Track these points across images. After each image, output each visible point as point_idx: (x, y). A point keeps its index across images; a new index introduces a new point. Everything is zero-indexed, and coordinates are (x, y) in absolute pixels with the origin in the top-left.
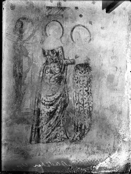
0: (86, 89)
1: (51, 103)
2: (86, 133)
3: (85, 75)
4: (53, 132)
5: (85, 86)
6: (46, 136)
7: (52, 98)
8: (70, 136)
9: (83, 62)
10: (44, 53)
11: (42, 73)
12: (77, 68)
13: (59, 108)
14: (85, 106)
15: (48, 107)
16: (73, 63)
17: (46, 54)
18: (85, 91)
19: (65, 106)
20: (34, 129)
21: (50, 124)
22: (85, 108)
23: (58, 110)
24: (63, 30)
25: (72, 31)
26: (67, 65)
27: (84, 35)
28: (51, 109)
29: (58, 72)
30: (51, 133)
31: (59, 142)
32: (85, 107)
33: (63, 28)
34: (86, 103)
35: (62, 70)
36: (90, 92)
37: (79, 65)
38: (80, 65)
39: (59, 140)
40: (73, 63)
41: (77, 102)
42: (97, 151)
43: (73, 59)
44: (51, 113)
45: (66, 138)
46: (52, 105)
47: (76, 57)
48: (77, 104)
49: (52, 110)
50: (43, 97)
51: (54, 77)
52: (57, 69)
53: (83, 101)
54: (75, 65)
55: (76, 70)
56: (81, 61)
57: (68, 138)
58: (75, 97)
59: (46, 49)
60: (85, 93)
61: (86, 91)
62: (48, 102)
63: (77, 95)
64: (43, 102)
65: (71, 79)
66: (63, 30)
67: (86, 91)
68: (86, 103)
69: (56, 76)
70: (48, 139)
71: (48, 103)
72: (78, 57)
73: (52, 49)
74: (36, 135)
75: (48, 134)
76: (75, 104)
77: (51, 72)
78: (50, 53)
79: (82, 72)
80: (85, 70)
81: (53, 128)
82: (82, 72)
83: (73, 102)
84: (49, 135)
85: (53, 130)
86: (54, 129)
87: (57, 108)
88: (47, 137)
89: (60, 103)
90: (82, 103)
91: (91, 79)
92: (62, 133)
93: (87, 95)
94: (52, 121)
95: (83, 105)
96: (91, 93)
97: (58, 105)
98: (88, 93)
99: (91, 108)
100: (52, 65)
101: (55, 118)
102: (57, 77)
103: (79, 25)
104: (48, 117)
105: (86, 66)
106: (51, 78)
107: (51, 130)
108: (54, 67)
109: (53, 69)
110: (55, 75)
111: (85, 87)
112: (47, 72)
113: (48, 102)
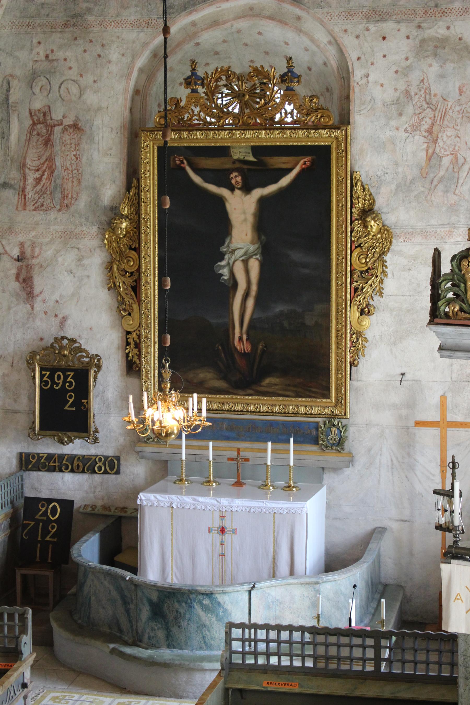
0: (75, 153)
1: (37, 168)
2: (73, 202)
3: (74, 137)
4: (40, 200)
5: (72, 149)
6: (33, 204)
7: (37, 163)
8: (57, 205)
9: (72, 123)
10: (31, 113)
11: (28, 135)
12: (64, 130)
13: (46, 174)
14: (74, 172)
15: (33, 172)
16: (60, 124)
17: (33, 114)
18: (72, 156)
19: (52, 172)
20: (20, 195)
21: (36, 191)
22: (74, 175)
23: (45, 177)
24: (50, 86)
25: (60, 87)
26: (54, 126)
27: (74, 90)
28: (37, 175)
29: (45, 134)
30: (37, 201)
31: (46, 210)
32: (75, 174)
33: (50, 84)
34: (75, 169)
35: (49, 132)
36: (78, 157)
37: (67, 125)
38: (69, 126)
39: (45, 209)
40: (60, 124)
41: (65, 168)
42: (85, 223)
43: (61, 120)
44: (37, 179)
45: (53, 206)
46: (38, 170)
47: (64, 117)
48: (65, 170)
49: (38, 176)
50: (28, 162)
51: (41, 139)
52: (45, 131)
53: (72, 166)
54: (63, 126)
55: (63, 132)
56: (68, 121)
57: (55, 207)
58: (62, 162)
59: (32, 108)
60: (74, 158)
61: (74, 155)
62: (34, 167)
63: (64, 159)
64: (29, 166)
65: (58, 142)
66: (50, 86)
67: (74, 155)
68: (75, 169)
69: (43, 138)
70: (34, 206)
71: (34, 168)
72: (66, 117)
73: (38, 108)
74: (23, 202)
75: (35, 202)
76: (63, 171)
77: (38, 134)
78: (37, 113)
79: (71, 134)
80: (74, 131)
81: (39, 196)
82: (71, 134)
83: (60, 168)
84: (36, 203)
85: (39, 198)
86: (41, 196)
87: (43, 175)
88: (34, 205)
89: (46, 167)
90: (71, 169)
91: (79, 142)
92: (49, 201)
93: (75, 160)
94: (39, 187)
95: (72, 172)
96: (79, 158)
97: (44, 171)
98: (77, 159)
99: (80, 175)
100: (39, 126)
101: (42, 184)
102: (44, 140)
103: (67, 80)
104: (35, 183)
105: (75, 127)
106: (38, 140)
107: (37, 198)
108: (41, 128)
109: (40, 131)
110: (42, 137)
111: (73, 151)
112: (33, 134)
113: (34, 167)
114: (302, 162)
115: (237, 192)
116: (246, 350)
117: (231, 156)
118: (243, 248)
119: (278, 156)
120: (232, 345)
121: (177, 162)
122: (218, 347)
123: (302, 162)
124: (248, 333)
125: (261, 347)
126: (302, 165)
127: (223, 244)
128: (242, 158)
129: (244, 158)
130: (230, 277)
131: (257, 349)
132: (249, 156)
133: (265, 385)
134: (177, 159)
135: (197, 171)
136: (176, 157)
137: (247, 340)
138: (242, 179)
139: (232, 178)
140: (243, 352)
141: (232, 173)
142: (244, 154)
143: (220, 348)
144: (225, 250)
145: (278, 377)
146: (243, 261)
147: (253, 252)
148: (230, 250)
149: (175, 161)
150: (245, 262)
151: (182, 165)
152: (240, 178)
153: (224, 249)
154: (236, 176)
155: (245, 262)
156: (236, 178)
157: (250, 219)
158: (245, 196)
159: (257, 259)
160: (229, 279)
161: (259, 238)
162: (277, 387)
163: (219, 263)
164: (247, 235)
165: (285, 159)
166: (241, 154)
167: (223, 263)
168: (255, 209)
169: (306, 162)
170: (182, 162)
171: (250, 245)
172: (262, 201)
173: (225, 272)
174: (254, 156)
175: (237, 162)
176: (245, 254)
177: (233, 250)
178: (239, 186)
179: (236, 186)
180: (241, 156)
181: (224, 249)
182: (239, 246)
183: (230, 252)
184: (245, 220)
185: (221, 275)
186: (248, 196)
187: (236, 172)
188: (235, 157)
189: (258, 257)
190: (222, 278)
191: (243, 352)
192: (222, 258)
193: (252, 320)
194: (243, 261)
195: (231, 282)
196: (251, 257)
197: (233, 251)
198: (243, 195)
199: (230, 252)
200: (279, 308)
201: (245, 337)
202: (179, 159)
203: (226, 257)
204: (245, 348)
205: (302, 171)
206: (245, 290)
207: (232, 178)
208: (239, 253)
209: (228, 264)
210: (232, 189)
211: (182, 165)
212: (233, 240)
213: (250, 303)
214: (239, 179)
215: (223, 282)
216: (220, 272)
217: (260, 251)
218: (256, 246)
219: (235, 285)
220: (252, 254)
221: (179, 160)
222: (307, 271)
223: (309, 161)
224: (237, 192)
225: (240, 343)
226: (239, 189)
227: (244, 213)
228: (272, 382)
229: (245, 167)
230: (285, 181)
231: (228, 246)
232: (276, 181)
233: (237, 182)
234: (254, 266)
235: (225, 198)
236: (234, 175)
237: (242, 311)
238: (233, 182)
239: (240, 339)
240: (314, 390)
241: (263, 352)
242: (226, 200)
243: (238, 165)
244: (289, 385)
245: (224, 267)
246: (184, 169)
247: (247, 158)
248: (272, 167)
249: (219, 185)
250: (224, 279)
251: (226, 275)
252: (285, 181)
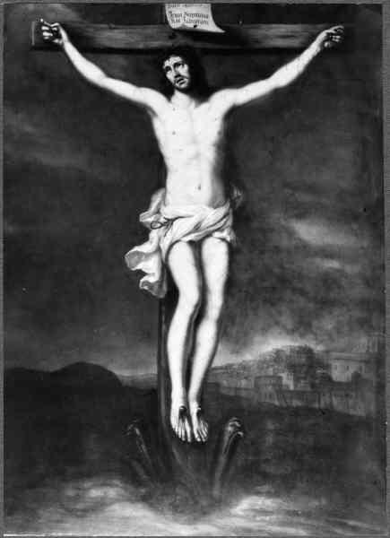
114: (323, 36)
115: (179, 98)
116: (196, 436)
117: (167, 23)
118: (190, 216)
119: (269, 22)
120: (165, 425)
121: (45, 34)
122: (133, 430)
123: (323, 36)
124: (201, 399)
125: (230, 429)
126: (324, 41)
127: (146, 206)
128: (191, 26)
129: (195, 26)
130: (162, 276)
131: (221, 433)
132: (207, 23)
133: (241, 513)
134: (44, 28)
135: (87, 50)
136: (43, 24)
137: (199, 414)
138: (190, 71)
139: (168, 68)
140: (189, 440)
141: (168, 58)
142: (195, 18)
143: (138, 431)
144: (151, 220)
145: (269, 495)
146: (191, 243)
147: (215, 224)
148: (162, 220)
149: (39, 32)
150: (196, 246)
151: (56, 41)
152: (186, 67)
153: (147, 218)
154: (176, 65)
155: (196, 246)
156: (177, 69)
157: (209, 155)
158: (196, 106)
159: (223, 240)
160: (160, 283)
161: (228, 195)
162: (268, 518)
163: (136, 249)
164: (200, 188)
165: (283, 29)
166: (187, 18)
167: (146, 248)
168: (219, 133)
169: (332, 34)
170: (58, 36)
171: (208, 209)
172: (234, 116)
173: (151, 269)
174: (218, 25)
175: (179, 36)
176: (197, 228)
177: (168, 220)
178: (183, 86)
179: (177, 85)
180: (190, 22)
181: (147, 218)
182: (182, 213)
183: (162, 225)
184: (197, 156)
185: (141, 274)
186: (205, 106)
187: (177, 55)
188: (174, 25)
189: (225, 234)
190: (142, 280)
191: (189, 440)
192: (142, 235)
193: (209, 371)
194: (191, 243)
195: (165, 288)
196: (209, 235)
197: (169, 223)
198: (193, 104)
199: (162, 225)
200: (272, 344)
201: (194, 408)
202: (50, 27)
203: (154, 235)
204: (195, 432)
205: (323, 53)
206: (196, 306)
207: (168, 68)
208: (180, 228)
209: (159, 250)
210: (167, 90)
211: (56, 41)
212: (169, 197)
213: (207, 332)
214: (184, 70)
215: (146, 288)
216: (139, 267)
217: (230, 223)
218: (222, 211)
219: (173, 294)
220: (212, 229)
221: (50, 31)
222: (334, 264)
223: (338, 34)
224: (179, 98)
225: (183, 421)
226: (184, 91)
227: (195, 141)
228: (257, 507)
229: (198, 45)
230: (286, 75)
231: (158, 212)
232: (265, 74)
233: (178, 75)
234: (217, 256)
235: (150, 109)
236: (170, 62)
237: (189, 352)
238: (171, 76)
239: (184, 413)
240: (351, 523)
241: (236, 441)
242: (154, 113)
243: (181, 41)
244: (295, 513)
245: (148, 256)
246: (60, 48)
247: (202, 27)
248: (257, 46)
249: (139, 83)
250: (147, 283)
251: (153, 274)
252: (286, 75)
